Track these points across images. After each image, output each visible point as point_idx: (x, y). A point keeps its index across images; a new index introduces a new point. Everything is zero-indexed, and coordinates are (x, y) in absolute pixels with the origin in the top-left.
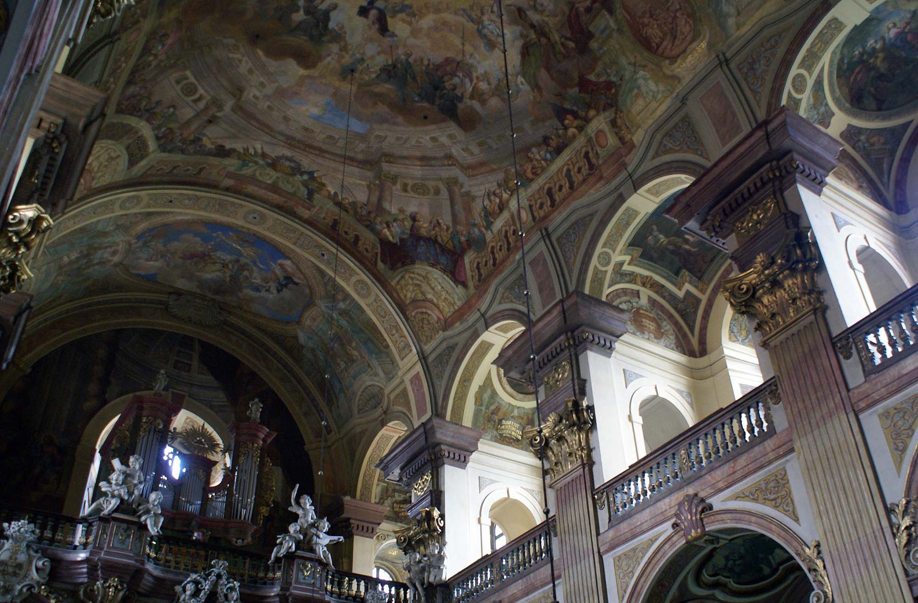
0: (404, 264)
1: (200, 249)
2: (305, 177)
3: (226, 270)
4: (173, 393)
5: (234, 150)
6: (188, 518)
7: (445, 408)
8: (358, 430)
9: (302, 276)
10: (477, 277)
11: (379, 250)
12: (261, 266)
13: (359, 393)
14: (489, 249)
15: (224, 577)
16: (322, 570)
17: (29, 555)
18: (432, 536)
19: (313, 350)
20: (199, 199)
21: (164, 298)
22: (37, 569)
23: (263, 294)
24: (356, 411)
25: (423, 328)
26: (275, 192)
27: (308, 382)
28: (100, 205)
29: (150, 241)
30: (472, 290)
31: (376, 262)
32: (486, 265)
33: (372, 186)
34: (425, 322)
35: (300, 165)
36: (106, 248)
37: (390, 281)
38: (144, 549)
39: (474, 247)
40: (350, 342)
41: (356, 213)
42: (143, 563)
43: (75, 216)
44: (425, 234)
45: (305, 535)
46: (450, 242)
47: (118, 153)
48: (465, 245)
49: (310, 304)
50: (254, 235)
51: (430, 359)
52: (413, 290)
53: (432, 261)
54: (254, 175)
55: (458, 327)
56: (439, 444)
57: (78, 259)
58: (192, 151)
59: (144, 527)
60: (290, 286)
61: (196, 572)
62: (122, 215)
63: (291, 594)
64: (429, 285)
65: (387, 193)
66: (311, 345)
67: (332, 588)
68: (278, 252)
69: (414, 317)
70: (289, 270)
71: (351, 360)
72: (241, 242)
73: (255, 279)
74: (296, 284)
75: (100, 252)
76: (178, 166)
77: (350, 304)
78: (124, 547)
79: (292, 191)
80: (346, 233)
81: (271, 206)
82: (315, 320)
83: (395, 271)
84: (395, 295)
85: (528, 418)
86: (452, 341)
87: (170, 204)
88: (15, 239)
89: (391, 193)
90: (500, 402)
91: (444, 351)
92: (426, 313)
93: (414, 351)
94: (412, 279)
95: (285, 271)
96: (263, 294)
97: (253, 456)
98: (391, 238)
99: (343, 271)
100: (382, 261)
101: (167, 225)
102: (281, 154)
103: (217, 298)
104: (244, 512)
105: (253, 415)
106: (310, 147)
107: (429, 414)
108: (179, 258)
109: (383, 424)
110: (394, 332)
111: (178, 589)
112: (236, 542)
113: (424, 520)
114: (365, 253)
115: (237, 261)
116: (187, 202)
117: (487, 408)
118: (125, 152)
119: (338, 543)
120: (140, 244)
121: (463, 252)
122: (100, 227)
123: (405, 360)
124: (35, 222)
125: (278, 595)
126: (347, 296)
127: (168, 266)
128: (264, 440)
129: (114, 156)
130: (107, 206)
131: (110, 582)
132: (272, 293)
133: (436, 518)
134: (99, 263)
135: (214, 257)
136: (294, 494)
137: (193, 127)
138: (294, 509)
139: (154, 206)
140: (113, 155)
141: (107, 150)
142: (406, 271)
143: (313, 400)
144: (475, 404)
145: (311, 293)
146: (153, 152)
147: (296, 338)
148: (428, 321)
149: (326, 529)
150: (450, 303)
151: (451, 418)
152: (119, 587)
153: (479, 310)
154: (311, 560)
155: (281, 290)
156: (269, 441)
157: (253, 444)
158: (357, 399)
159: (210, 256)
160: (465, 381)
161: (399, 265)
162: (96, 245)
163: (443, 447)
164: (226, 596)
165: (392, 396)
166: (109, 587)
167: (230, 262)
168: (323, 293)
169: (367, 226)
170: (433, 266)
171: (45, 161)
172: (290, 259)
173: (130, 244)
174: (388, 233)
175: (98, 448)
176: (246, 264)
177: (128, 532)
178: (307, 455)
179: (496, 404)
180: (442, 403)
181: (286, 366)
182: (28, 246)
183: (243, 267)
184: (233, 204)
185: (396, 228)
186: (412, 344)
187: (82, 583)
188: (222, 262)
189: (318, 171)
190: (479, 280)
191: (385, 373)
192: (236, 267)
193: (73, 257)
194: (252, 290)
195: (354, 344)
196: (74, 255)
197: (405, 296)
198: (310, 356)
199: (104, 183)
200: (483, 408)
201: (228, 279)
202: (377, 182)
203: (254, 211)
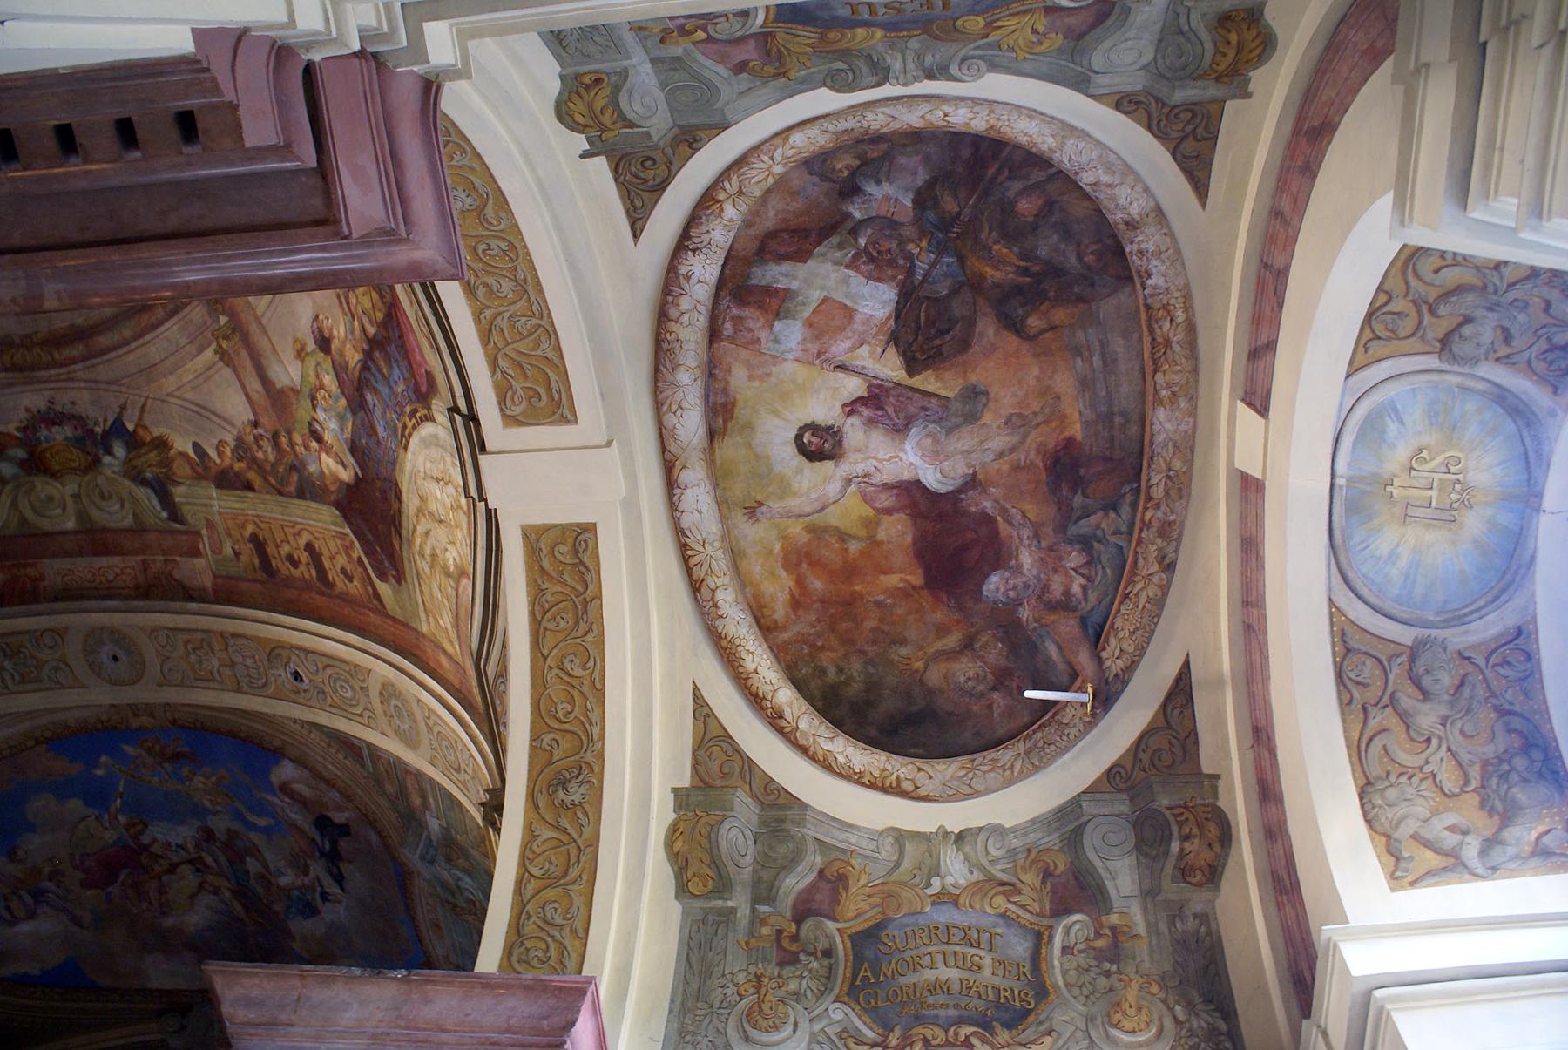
1: (110, 836)
2: (119, 450)
12: (262, 822)
26: (106, 551)
33: (225, 344)
35: (80, 418)
54: (24, 521)
65: (253, 329)
73: (281, 874)
79: (129, 521)
85: (1047, 874)
89: (258, 320)
90: (836, 838)
100: (383, 577)
102: (23, 414)
106: (56, 341)
108: (85, 885)
117: (763, 892)
135: (155, 849)
144: (682, 890)
159: (146, 848)
160: (563, 783)
161: (396, 543)
169: (301, 495)
179: (814, 860)
189: (123, 407)
192: (222, 859)
200: (739, 901)
201: (238, 908)
202: (223, 319)
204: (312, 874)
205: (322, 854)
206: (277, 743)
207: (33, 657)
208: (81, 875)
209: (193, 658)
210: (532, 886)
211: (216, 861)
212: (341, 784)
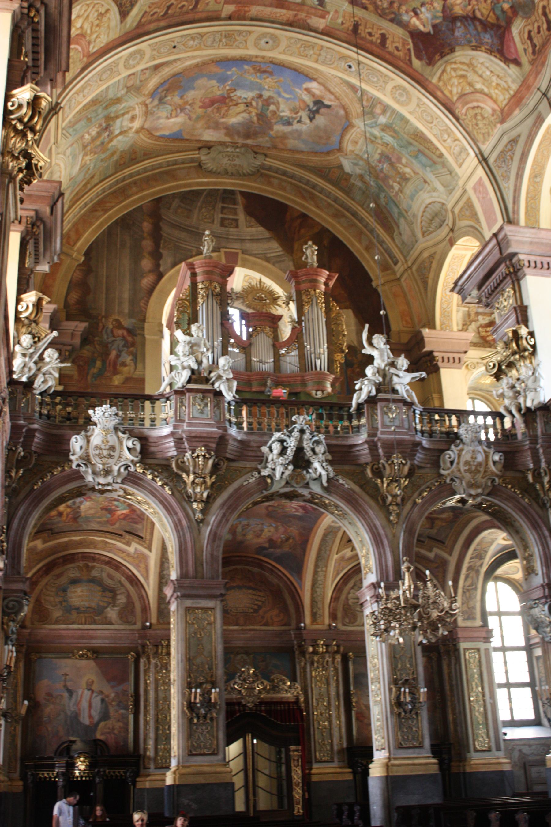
0: (442, 56)
1: (219, 93)
3: (250, 109)
6: (263, 377)
7: (516, 212)
8: (426, 255)
9: (332, 97)
10: (530, 50)
11: (411, 46)
13: (420, 214)
14: (540, 11)
15: (307, 432)
16: (408, 410)
17: (118, 437)
18: (523, 357)
19: (361, 177)
20: (202, 37)
21: (195, 155)
22: (129, 449)
23: (296, 126)
24: (419, 235)
25: (477, 125)
27: (363, 213)
28: (104, 71)
29: (165, 97)
30: (527, 67)
31: (410, 60)
32: (539, 32)
34: (479, 117)
36: (123, 115)
37: (430, 79)
38: (224, 415)
39: (520, 13)
40: (399, 159)
41: (376, 7)
42: (225, 429)
43: (83, 88)
44: (461, 12)
45: (384, 376)
46: (491, 14)
47: (106, 7)
48: (510, 13)
49: (348, 126)
50: (271, 62)
51: (491, 161)
52: (459, 83)
53: (474, 44)
55: (518, 115)
56: (515, 254)
57: (99, 134)
59: (219, 394)
60: (323, 110)
61: (279, 430)
62: (129, 76)
63: (379, 439)
64: (475, 72)
66: (358, 171)
67: (422, 427)
69: (466, 115)
70: (317, 92)
71: (405, 179)
72: (258, 74)
73: (283, 111)
74: (328, 107)
75: (118, 122)
76: (172, 4)
77: (391, 116)
78: (204, 416)
80: (370, 34)
81: (282, 24)
82: (356, 143)
83: (433, 65)
84: (439, 94)
86: (514, 134)
87: (174, 50)
88: (20, 127)
91: (506, 146)
92: (478, 107)
93: (472, 154)
94: (455, 70)
95: (313, 95)
96: (296, 126)
97: (317, 304)
98: (421, 28)
99: (375, 79)
100: (419, 57)
101: (179, 74)
103: (249, 142)
105: (309, 260)
107: (500, 222)
108: (201, 107)
109: (452, 243)
110: (446, 136)
111: (265, 449)
112: (316, 395)
113: (512, 340)
114: (396, 52)
115: (260, 96)
116: (191, 43)
119: (422, 380)
120: (156, 102)
121: (509, 22)
122: (111, 95)
123: (464, 166)
124: (34, 102)
125: (366, 442)
126: (386, 108)
127: (190, 119)
128: (326, 284)
129: (103, 12)
130: (111, 70)
131: (198, 452)
132: (305, 124)
133: (524, 336)
134: (121, 133)
135: (235, 98)
136: (365, 335)
138: (368, 350)
139: (159, 58)
140: (102, 10)
141: (93, 7)
142: (446, 62)
143: (372, 231)
145: (347, 114)
147: (340, 167)
148: (482, 115)
149: (406, 367)
150: (504, 89)
151: (526, 222)
152: (207, 456)
153: (538, 89)
154: (395, 401)
155: (314, 118)
156: (331, 284)
157: (315, 290)
158: (419, 221)
159: (230, 97)
160: (536, 177)
161: (437, 57)
162: (112, 115)
163: (521, 257)
164: (313, 450)
165: (457, 210)
166: (198, 457)
167: (253, 99)
168: (359, 110)
169: (392, 21)
170: (476, 48)
171: (28, 34)
172: (315, 80)
174: (417, 23)
175: (164, 322)
176: (270, 97)
177: (205, 401)
178: (375, 291)
180: (514, 208)
181: (336, 200)
182: (33, 130)
183: (268, 102)
184: (240, 33)
185: (425, 14)
186: (468, 147)
187: (172, 457)
188: (245, 101)
190: (534, 53)
191: (444, 186)
192: (260, 104)
193: (94, 133)
194: (284, 124)
195: (404, 161)
196: (94, 131)
197: (451, 92)
198: (359, 184)
199: (102, 45)
201: (255, 119)
203: (264, 35)
204: (299, 114)
205: (309, 110)
206: (315, 77)
207: (235, 38)
208: (201, 104)
209: (302, 49)
210: (529, 199)
211: (257, 104)
212: (338, 95)
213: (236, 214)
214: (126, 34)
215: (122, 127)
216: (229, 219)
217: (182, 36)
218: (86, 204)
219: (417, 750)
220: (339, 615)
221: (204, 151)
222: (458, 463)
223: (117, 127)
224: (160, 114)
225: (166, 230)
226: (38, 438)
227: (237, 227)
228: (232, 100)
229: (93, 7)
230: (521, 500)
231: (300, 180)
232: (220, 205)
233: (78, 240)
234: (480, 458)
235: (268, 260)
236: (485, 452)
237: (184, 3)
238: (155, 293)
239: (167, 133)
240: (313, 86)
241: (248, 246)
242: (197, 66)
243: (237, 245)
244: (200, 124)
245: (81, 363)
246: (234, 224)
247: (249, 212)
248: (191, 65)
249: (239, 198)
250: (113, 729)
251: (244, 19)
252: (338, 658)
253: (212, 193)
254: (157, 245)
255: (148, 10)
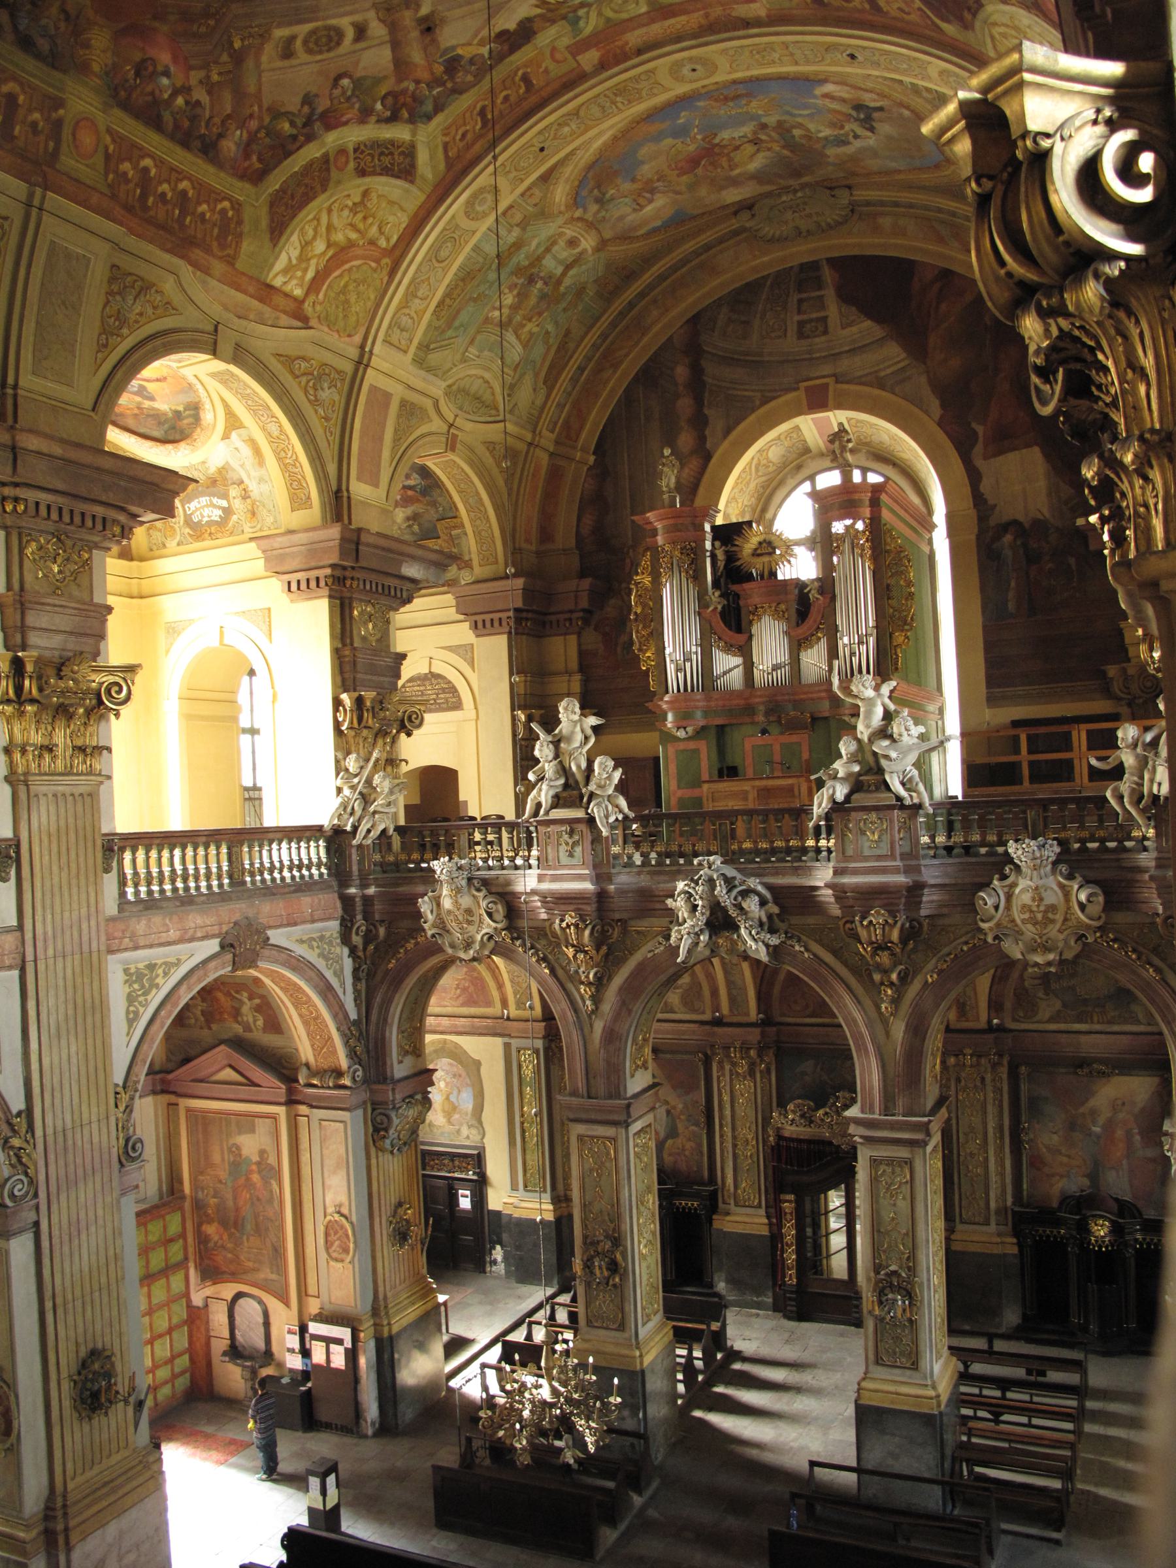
4: (807, 389)
5: (529, 20)
21: (735, 224)
28: (435, 250)
54: (608, 20)
57: (522, 296)
58: (470, 78)
68: (809, 82)
74: (881, 109)
81: (694, 36)
96: (858, 144)
104: (855, 661)
116: (566, 129)
118: (368, 180)
120: (594, 208)
130: (452, 237)
131: (568, 919)
137: (417, 56)
146: (414, 134)
167: (755, 133)
172: (825, 81)
173: (580, 219)
183: (781, 127)
194: (838, 146)
213: (823, 307)
214: (436, 186)
215: (560, 262)
216: (811, 321)
217: (540, 133)
218: (581, 369)
219: (908, 1372)
220: (1008, 1005)
221: (745, 215)
222: (1008, 907)
223: (550, 264)
224: (617, 214)
225: (712, 370)
226: (377, 906)
227: (825, 332)
228: (725, 146)
229: (330, 211)
230: (1141, 970)
231: (926, 208)
232: (795, 297)
233: (581, 428)
234: (1053, 897)
235: (881, 384)
236: (1062, 887)
237: (504, 93)
238: (701, 490)
239: (658, 223)
240: (829, 88)
241: (844, 364)
242: (615, 139)
243: (827, 369)
244: (703, 191)
245: (607, 629)
246: (821, 329)
247: (845, 297)
248: (604, 144)
249: (828, 274)
250: (683, 1150)
251: (626, 57)
252: (1004, 1072)
253: (780, 279)
254: (699, 401)
255: (447, 139)
